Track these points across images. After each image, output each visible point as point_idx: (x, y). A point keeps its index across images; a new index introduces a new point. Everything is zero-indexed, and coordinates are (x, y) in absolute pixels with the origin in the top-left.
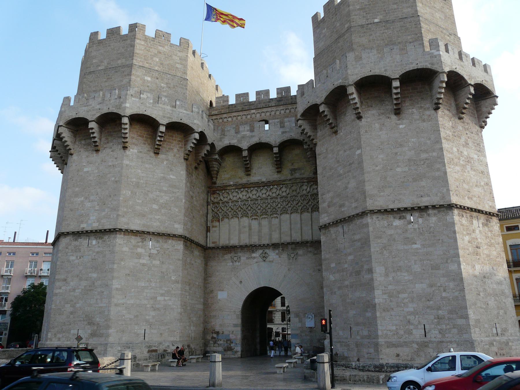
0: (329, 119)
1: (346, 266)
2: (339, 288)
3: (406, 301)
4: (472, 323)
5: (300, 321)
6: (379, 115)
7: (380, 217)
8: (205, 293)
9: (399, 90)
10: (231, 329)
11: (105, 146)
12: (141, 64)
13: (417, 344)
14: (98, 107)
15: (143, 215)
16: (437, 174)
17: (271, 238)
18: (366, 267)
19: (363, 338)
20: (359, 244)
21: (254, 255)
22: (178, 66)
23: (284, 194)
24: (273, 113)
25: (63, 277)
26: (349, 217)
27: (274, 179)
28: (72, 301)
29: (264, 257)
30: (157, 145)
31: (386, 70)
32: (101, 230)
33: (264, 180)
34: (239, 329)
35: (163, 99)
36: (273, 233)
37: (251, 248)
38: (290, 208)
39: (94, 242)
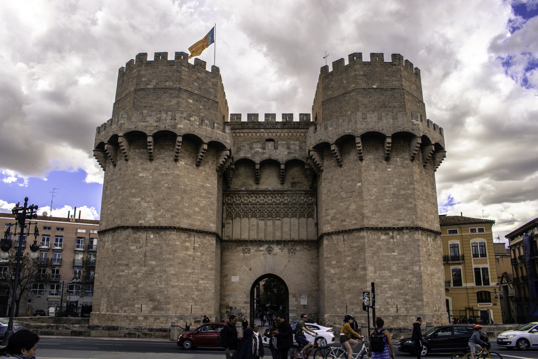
0: (337, 156)
1: (345, 264)
2: (338, 279)
3: (386, 289)
4: (425, 304)
5: (296, 300)
6: (375, 160)
7: (373, 232)
8: (221, 277)
9: (390, 145)
10: (242, 305)
11: (158, 157)
12: (185, 88)
13: (392, 317)
14: (155, 124)
15: (188, 216)
16: (410, 206)
17: (274, 236)
18: (361, 266)
19: (356, 313)
20: (355, 250)
21: (261, 248)
22: (211, 90)
23: (286, 202)
24: (278, 134)
25: (125, 262)
26: (350, 230)
27: (279, 189)
28: (134, 282)
29: (270, 251)
30: (200, 159)
31: (383, 129)
32: (158, 227)
33: (270, 189)
34: (249, 305)
35: (206, 121)
36: (276, 232)
37: (259, 243)
38: (290, 214)
39: (152, 236)
